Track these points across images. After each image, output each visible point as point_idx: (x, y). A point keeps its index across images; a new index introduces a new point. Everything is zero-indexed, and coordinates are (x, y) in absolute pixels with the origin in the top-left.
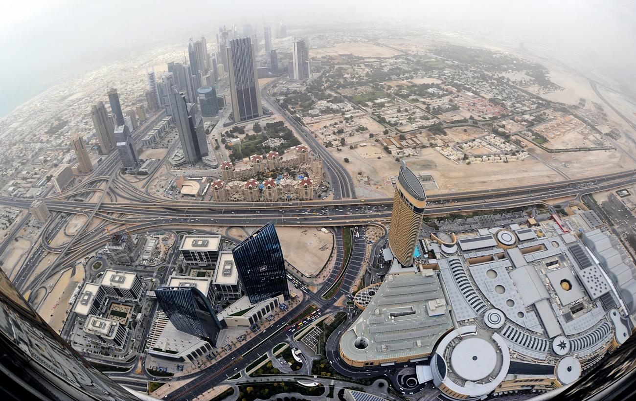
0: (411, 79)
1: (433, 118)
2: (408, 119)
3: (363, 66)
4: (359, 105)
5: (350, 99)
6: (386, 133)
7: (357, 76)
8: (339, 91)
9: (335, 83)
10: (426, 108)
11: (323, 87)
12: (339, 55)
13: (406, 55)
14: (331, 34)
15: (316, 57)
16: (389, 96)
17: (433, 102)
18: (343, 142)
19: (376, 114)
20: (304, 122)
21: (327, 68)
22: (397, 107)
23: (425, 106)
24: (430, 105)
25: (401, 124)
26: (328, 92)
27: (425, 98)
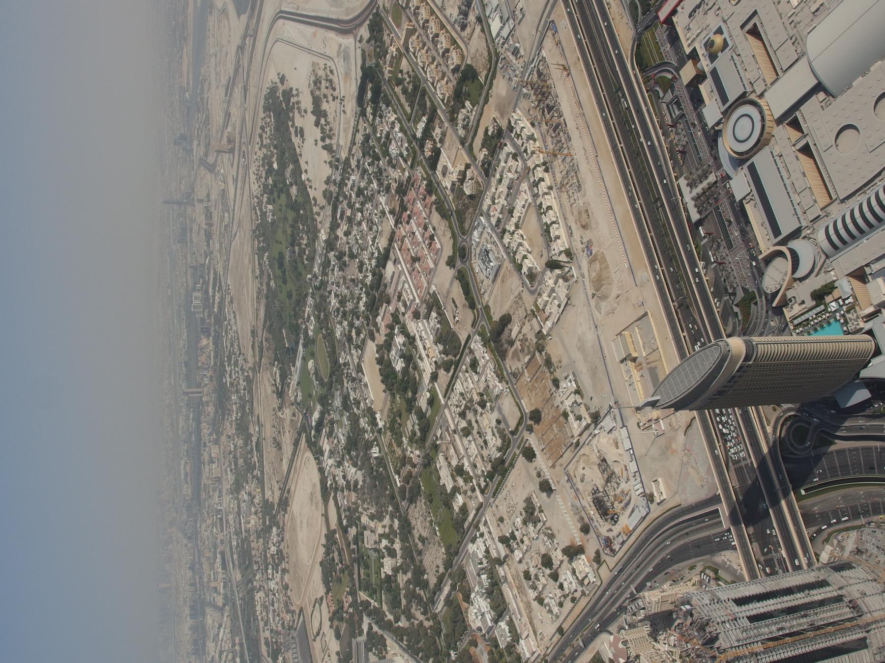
0: (375, 413)
1: (471, 352)
2: (483, 406)
3: (353, 531)
4: (466, 525)
5: (453, 552)
6: (530, 455)
7: (384, 542)
8: (433, 581)
9: (412, 596)
10: (448, 370)
11: (427, 624)
12: (327, 593)
13: (306, 432)
14: (262, 624)
15: (338, 653)
16: (429, 462)
17: (428, 356)
18: (573, 552)
19: (483, 484)
20: (536, 655)
21: (366, 621)
22: (456, 437)
23: (442, 372)
24: (436, 362)
25: (498, 422)
26: (440, 607)
27: (421, 376)
